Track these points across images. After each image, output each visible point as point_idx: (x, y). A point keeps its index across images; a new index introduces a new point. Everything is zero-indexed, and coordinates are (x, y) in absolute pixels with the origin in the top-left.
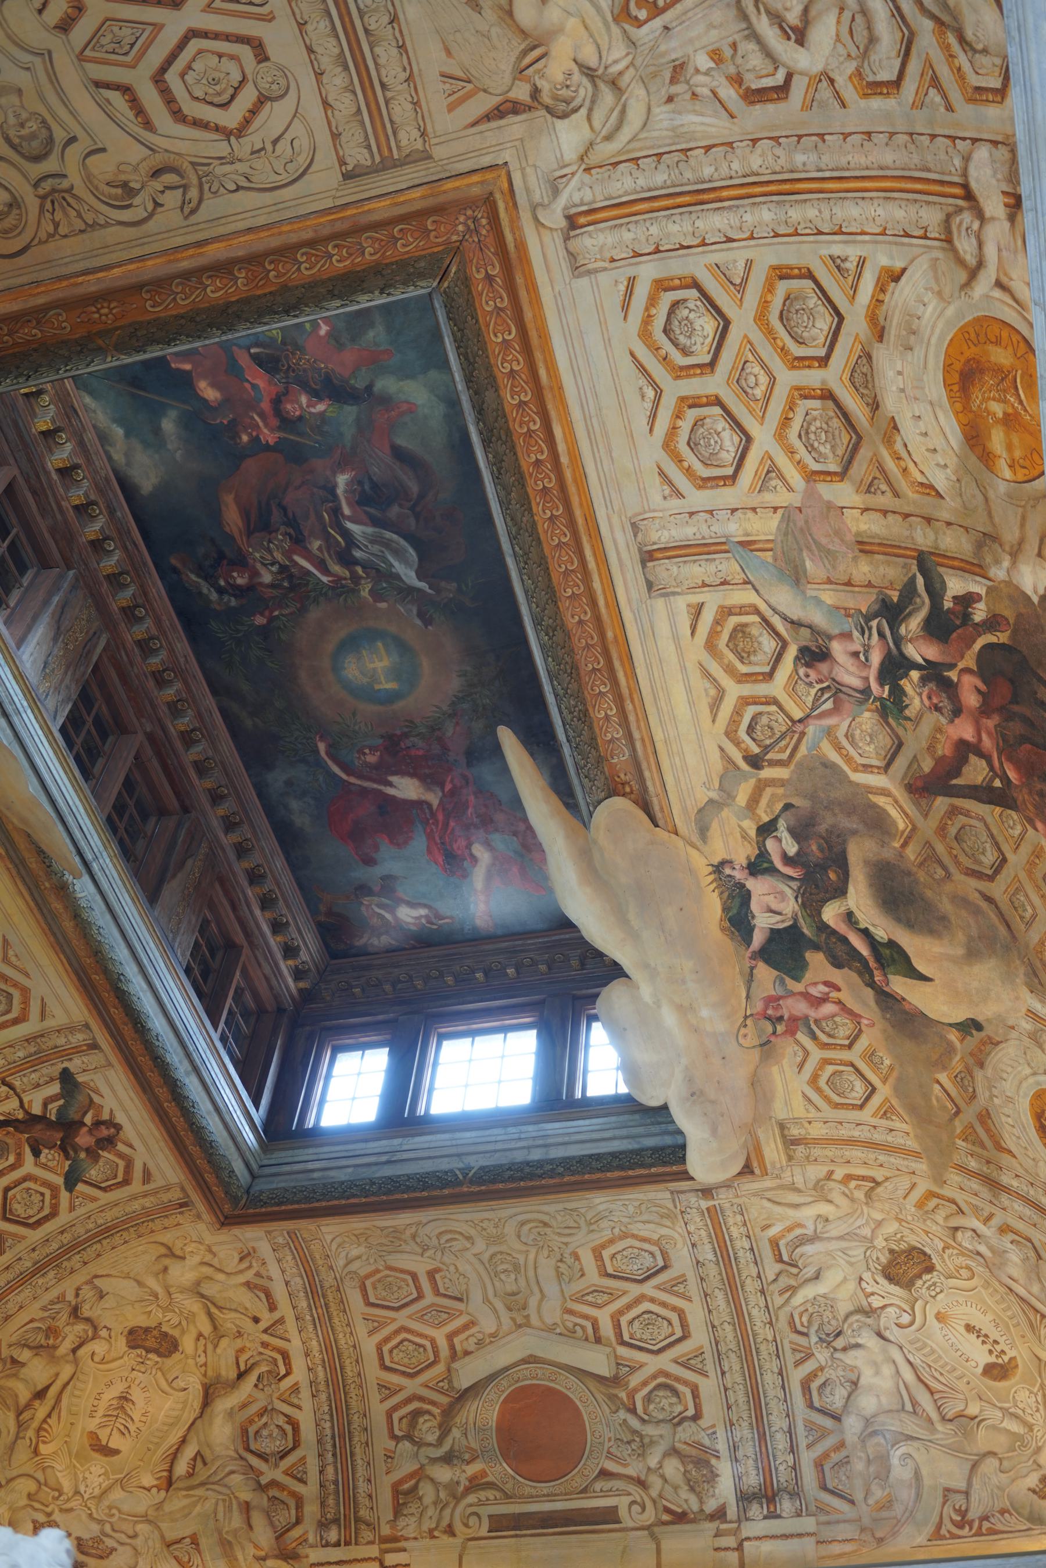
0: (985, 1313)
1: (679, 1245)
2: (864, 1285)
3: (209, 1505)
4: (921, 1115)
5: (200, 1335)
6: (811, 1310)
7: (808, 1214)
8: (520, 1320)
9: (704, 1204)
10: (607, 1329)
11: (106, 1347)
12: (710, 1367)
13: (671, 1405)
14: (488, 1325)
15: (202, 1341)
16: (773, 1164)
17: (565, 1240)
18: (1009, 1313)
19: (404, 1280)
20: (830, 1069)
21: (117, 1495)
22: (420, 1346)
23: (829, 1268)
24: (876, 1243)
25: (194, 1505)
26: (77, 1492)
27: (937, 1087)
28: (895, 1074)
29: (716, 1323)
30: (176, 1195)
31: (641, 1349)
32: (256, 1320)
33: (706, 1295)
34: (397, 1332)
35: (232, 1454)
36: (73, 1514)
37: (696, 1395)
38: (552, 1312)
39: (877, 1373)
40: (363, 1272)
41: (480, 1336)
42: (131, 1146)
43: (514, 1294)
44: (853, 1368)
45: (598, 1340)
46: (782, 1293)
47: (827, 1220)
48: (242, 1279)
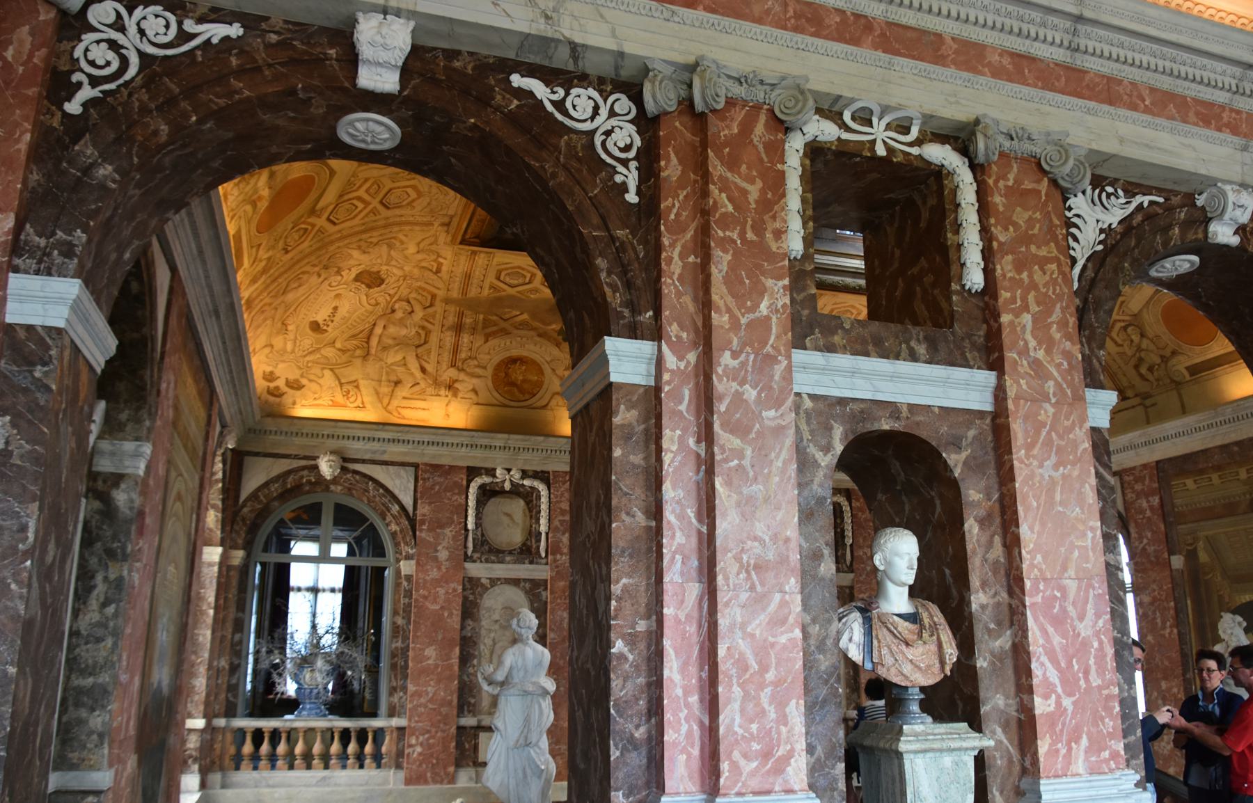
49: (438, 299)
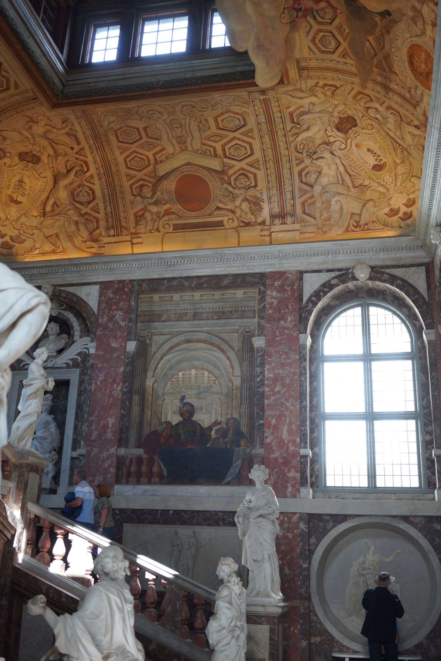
0: (376, 144)
1: (251, 116)
2: (327, 132)
3: (61, 222)
4: (359, 56)
5: (49, 155)
6: (304, 143)
7: (306, 101)
8: (183, 148)
9: (262, 97)
10: (220, 151)
11: (10, 161)
12: (261, 166)
13: (245, 181)
14: (170, 150)
15: (50, 158)
16: (293, 79)
17: (202, 113)
18: (386, 144)
19: (134, 131)
20: (321, 34)
21: (23, 219)
22: (142, 159)
23: (313, 125)
24: (334, 114)
25: (55, 222)
26: (7, 219)
27: (368, 43)
28: (350, 37)
29: (265, 149)
30: (30, 94)
31: (233, 159)
32: (72, 149)
33: (261, 137)
34: (132, 153)
35: (68, 202)
36: (7, 227)
37: (255, 178)
38: (197, 144)
39: (329, 168)
40: (116, 128)
41: (167, 155)
42: (7, 72)
43: (180, 137)
44: (320, 167)
45: (216, 156)
46: (293, 136)
47: (314, 104)
48: (64, 131)
49: (362, 91)
